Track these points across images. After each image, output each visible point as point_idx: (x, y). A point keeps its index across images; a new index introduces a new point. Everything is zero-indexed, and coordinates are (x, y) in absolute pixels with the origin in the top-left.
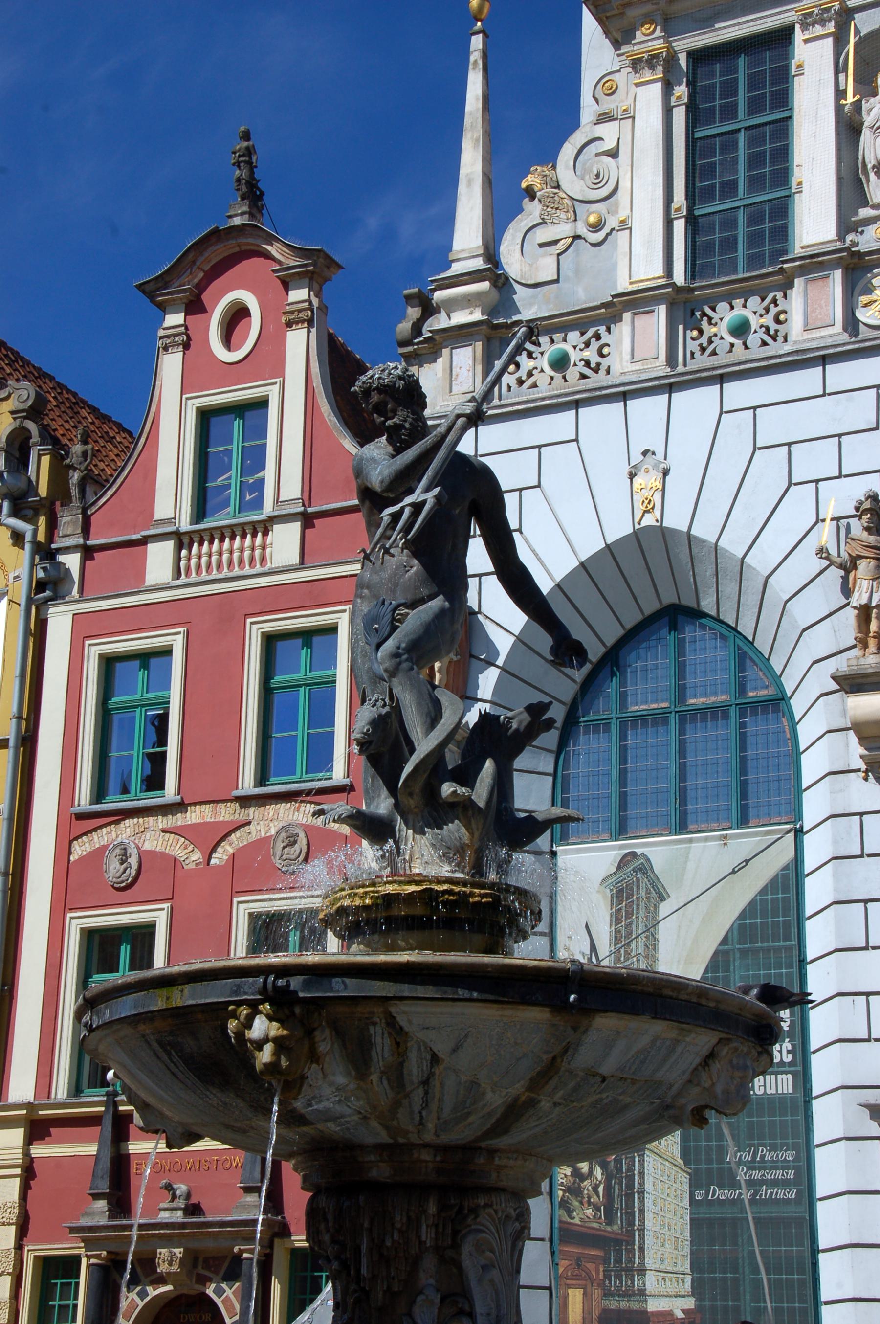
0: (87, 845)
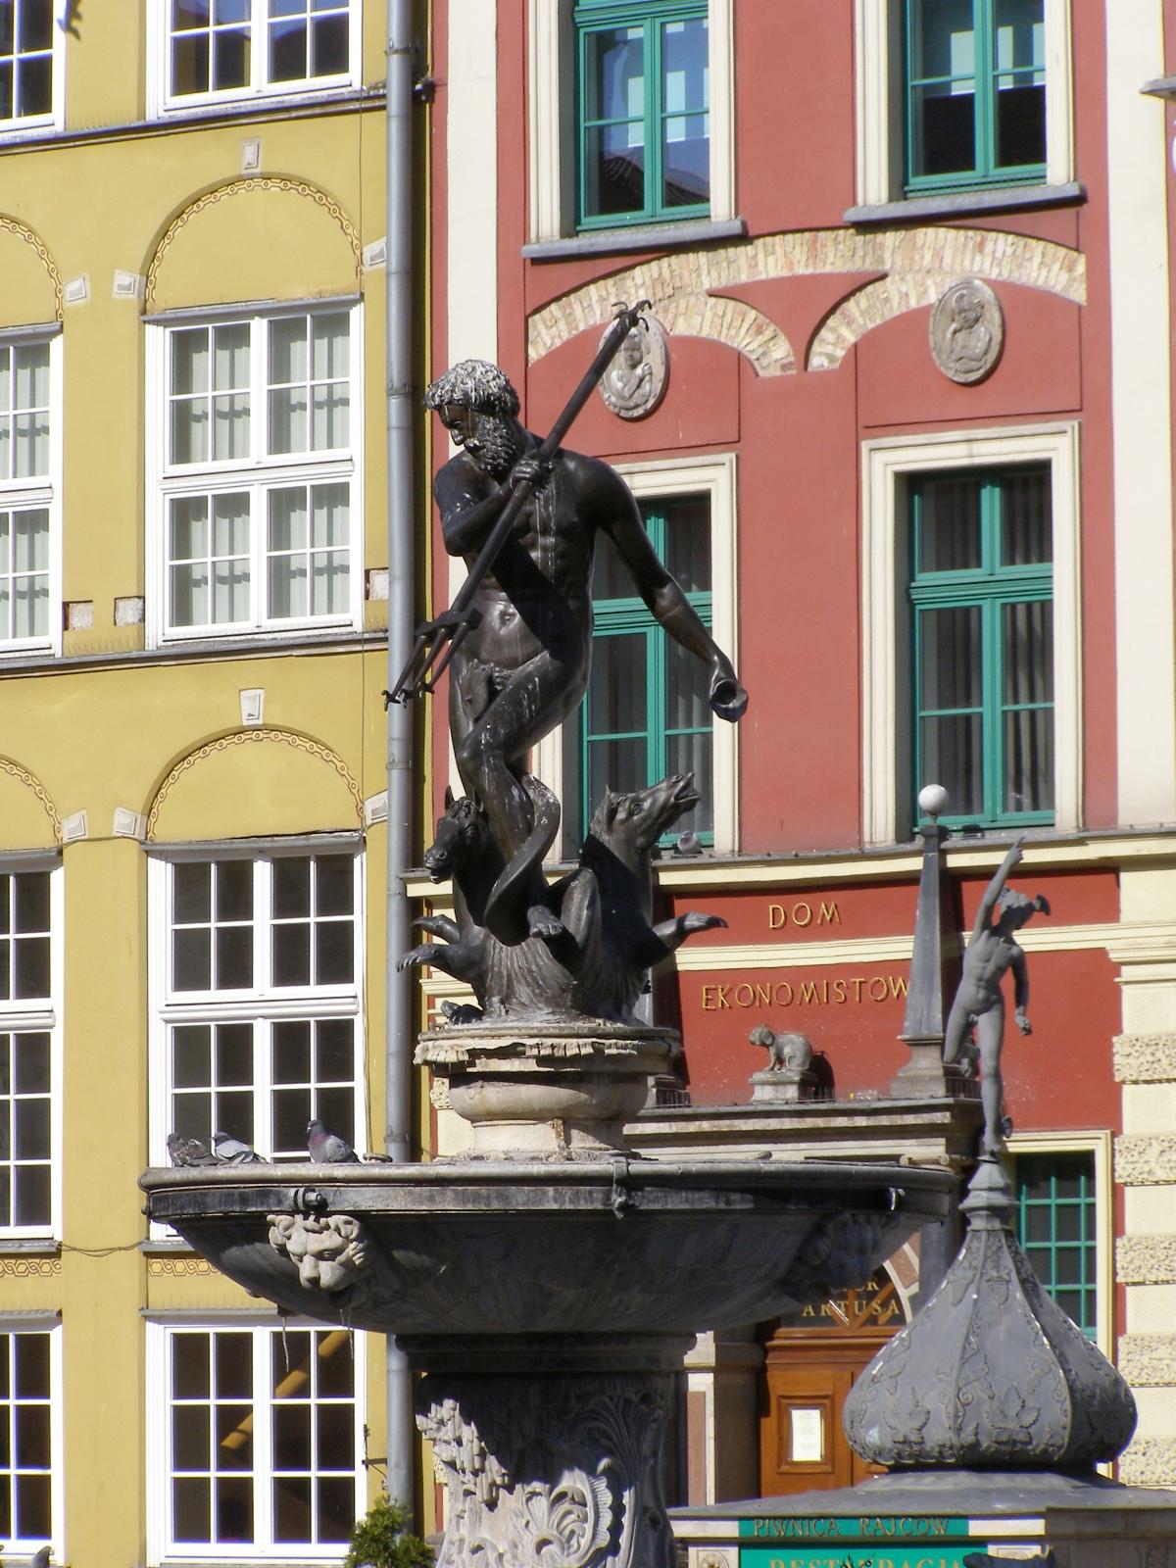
0: (562, 325)
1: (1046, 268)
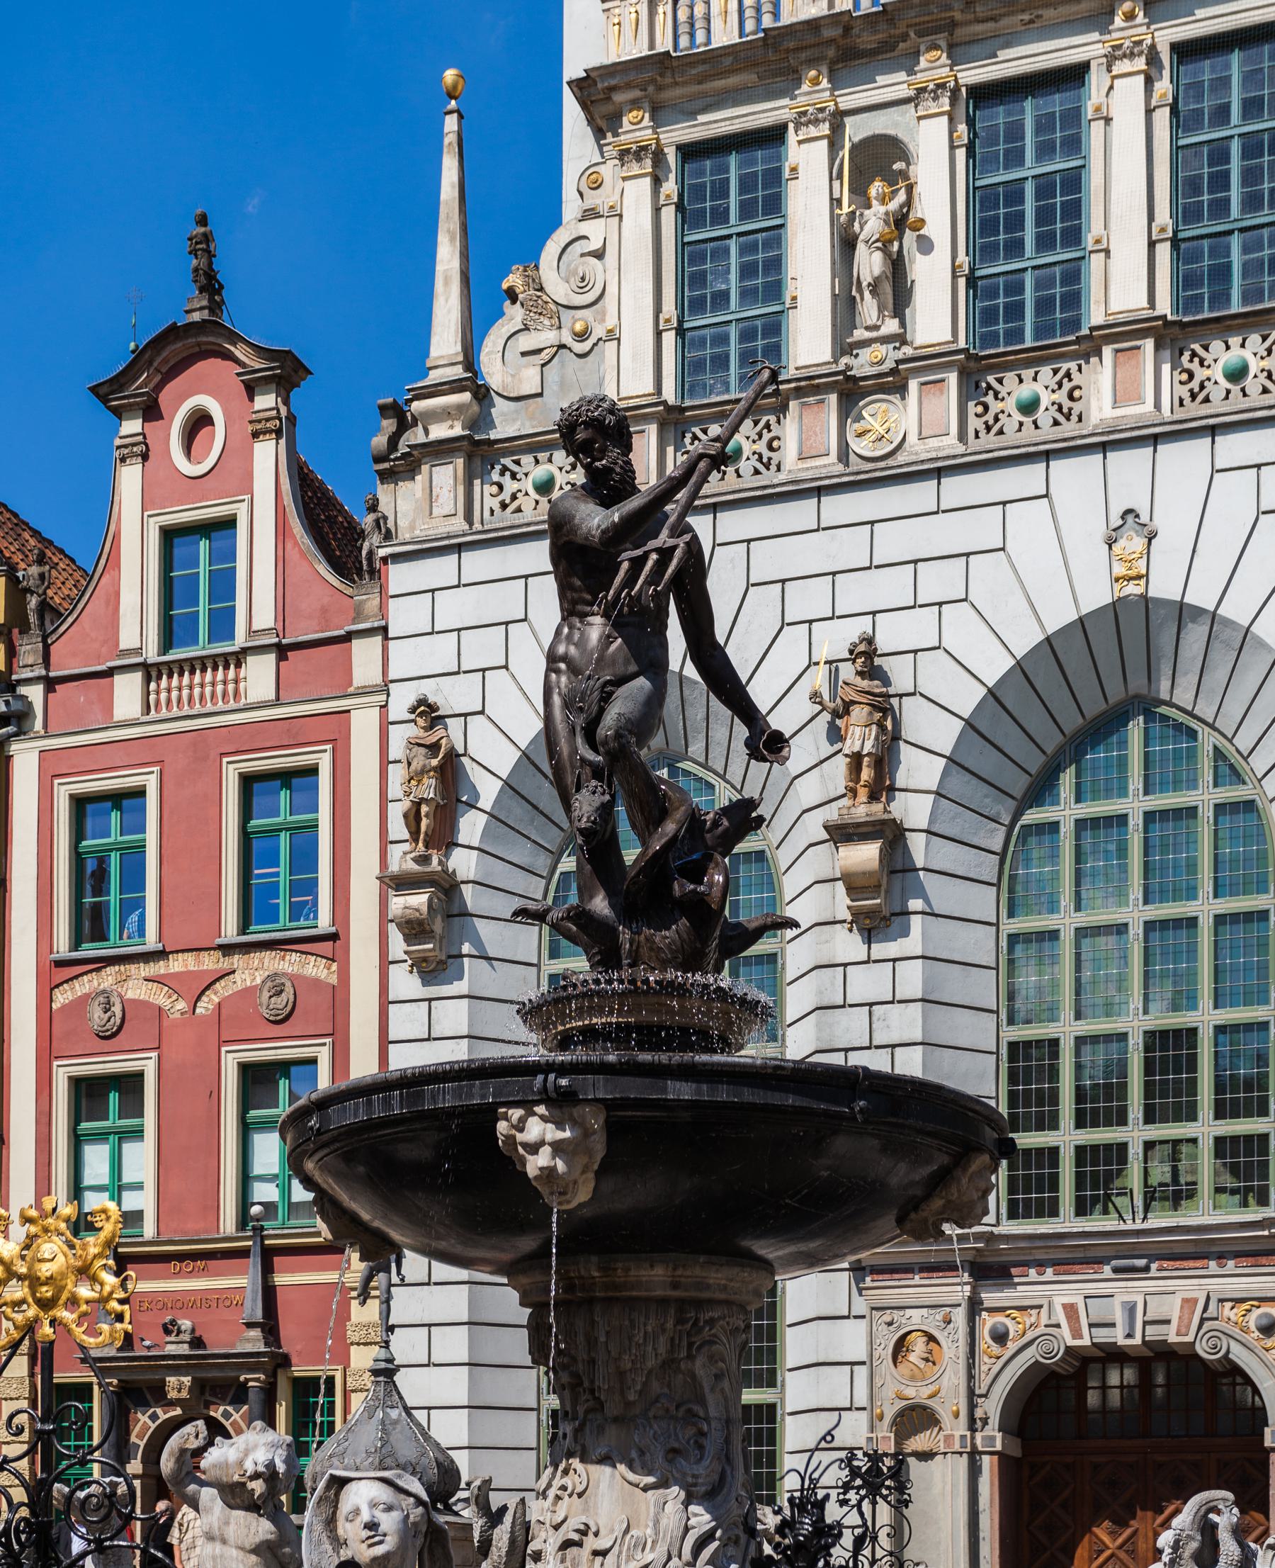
0: (69, 993)
1: (316, 968)
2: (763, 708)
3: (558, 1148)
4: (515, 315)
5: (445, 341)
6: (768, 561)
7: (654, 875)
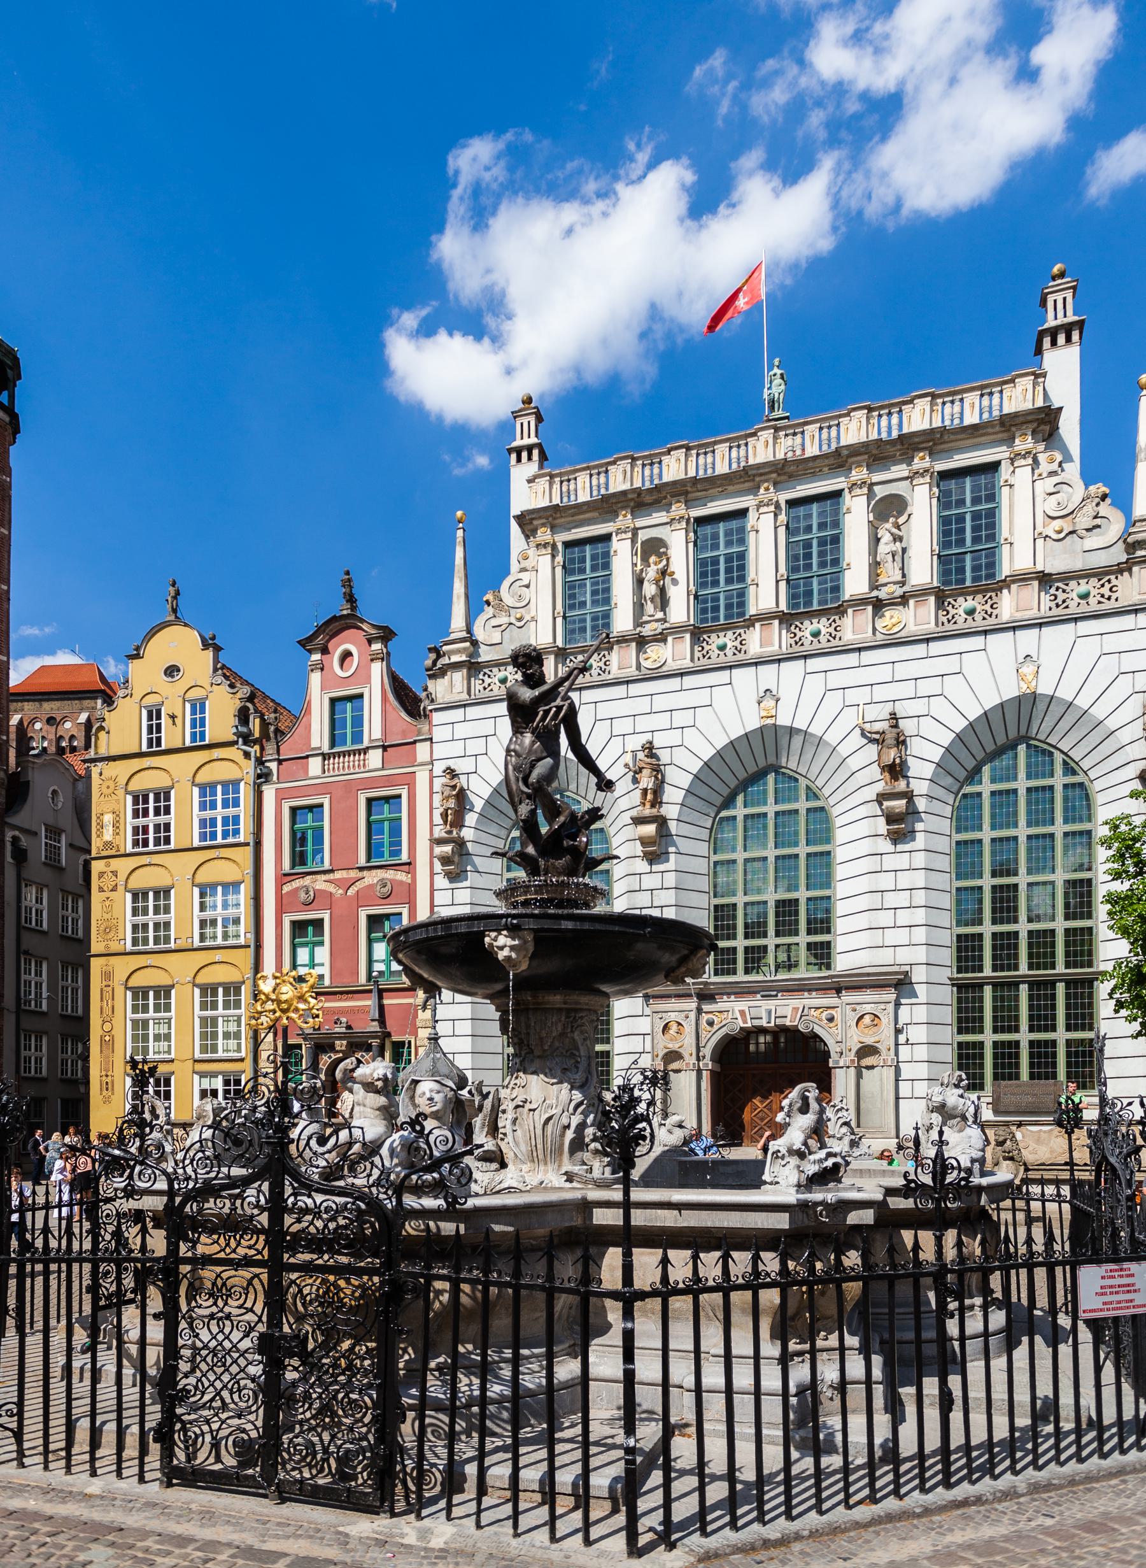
2: (603, 768)
3: (512, 948)
4: (489, 611)
5: (458, 621)
6: (604, 710)
7: (554, 837)
